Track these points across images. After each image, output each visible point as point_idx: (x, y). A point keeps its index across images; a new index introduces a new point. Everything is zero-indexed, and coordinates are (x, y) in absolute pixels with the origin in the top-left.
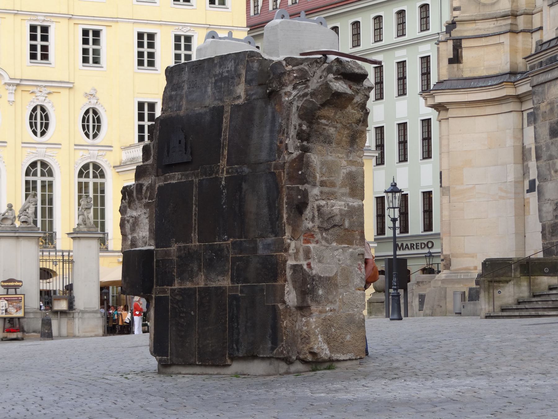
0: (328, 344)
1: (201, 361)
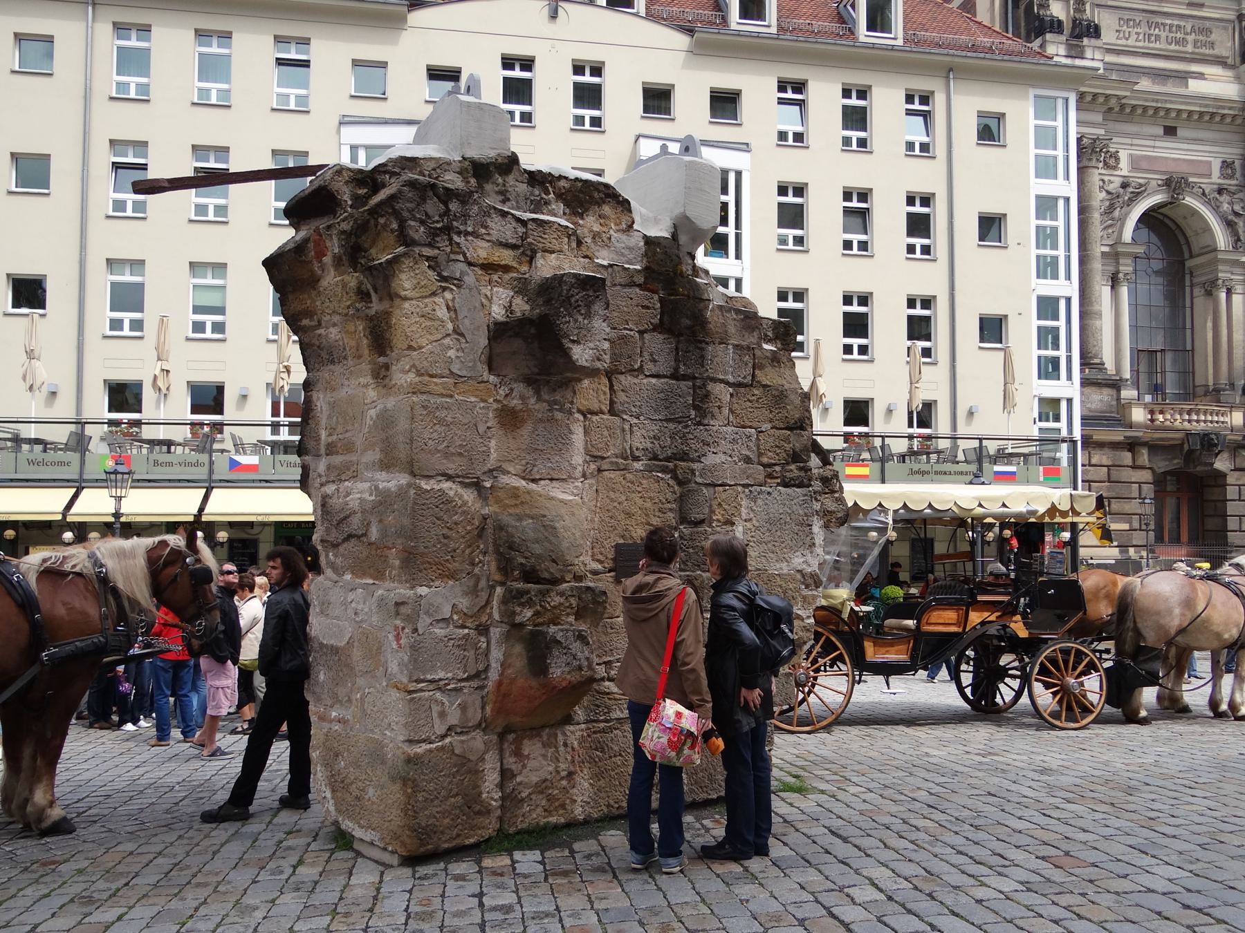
0: (333, 791)
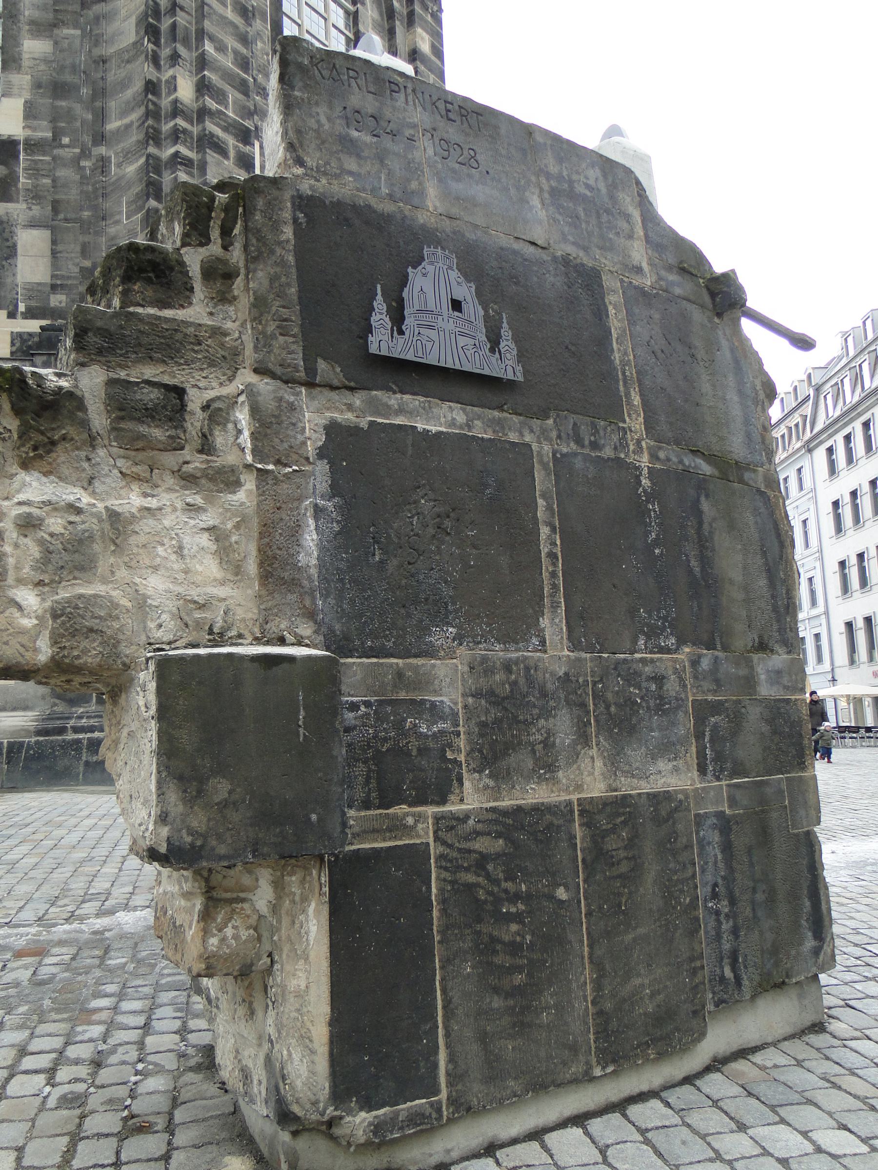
1: (614, 1061)
